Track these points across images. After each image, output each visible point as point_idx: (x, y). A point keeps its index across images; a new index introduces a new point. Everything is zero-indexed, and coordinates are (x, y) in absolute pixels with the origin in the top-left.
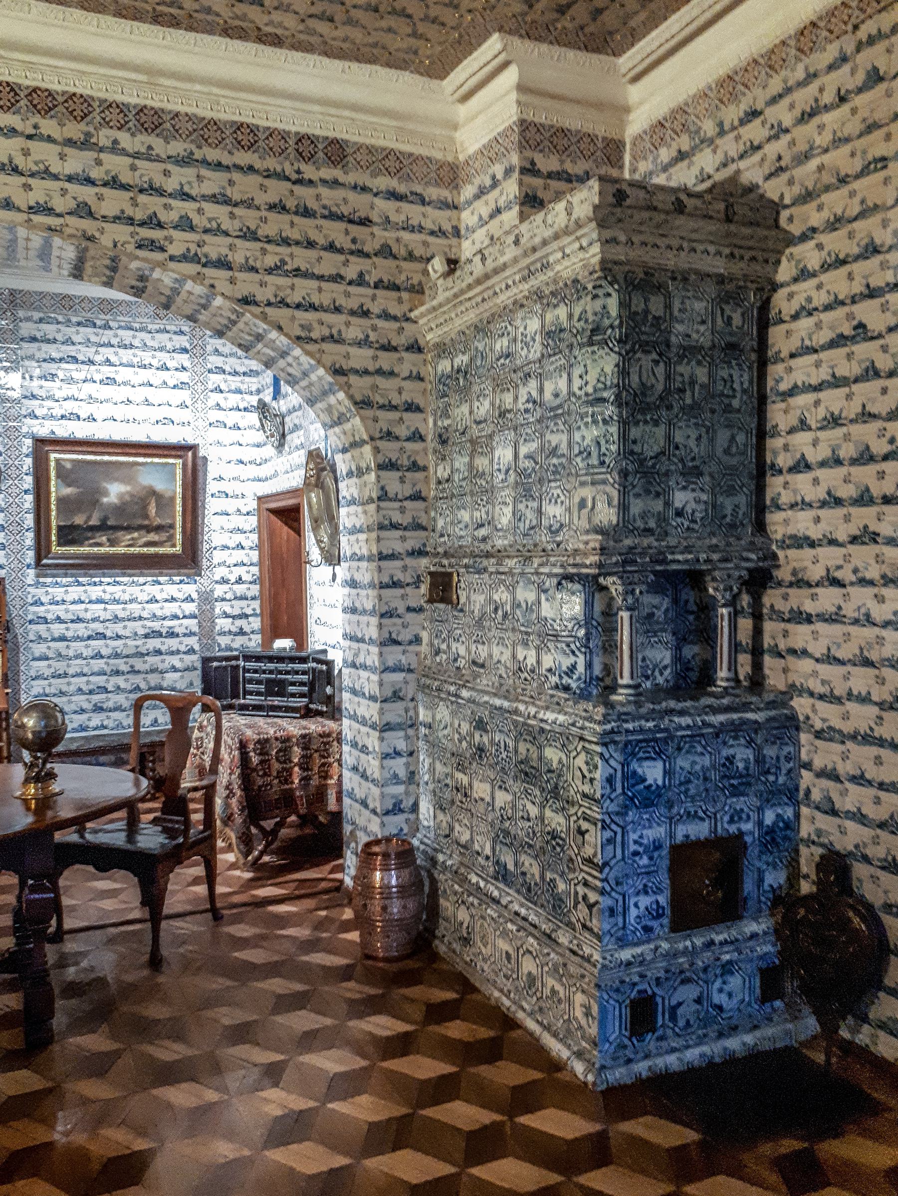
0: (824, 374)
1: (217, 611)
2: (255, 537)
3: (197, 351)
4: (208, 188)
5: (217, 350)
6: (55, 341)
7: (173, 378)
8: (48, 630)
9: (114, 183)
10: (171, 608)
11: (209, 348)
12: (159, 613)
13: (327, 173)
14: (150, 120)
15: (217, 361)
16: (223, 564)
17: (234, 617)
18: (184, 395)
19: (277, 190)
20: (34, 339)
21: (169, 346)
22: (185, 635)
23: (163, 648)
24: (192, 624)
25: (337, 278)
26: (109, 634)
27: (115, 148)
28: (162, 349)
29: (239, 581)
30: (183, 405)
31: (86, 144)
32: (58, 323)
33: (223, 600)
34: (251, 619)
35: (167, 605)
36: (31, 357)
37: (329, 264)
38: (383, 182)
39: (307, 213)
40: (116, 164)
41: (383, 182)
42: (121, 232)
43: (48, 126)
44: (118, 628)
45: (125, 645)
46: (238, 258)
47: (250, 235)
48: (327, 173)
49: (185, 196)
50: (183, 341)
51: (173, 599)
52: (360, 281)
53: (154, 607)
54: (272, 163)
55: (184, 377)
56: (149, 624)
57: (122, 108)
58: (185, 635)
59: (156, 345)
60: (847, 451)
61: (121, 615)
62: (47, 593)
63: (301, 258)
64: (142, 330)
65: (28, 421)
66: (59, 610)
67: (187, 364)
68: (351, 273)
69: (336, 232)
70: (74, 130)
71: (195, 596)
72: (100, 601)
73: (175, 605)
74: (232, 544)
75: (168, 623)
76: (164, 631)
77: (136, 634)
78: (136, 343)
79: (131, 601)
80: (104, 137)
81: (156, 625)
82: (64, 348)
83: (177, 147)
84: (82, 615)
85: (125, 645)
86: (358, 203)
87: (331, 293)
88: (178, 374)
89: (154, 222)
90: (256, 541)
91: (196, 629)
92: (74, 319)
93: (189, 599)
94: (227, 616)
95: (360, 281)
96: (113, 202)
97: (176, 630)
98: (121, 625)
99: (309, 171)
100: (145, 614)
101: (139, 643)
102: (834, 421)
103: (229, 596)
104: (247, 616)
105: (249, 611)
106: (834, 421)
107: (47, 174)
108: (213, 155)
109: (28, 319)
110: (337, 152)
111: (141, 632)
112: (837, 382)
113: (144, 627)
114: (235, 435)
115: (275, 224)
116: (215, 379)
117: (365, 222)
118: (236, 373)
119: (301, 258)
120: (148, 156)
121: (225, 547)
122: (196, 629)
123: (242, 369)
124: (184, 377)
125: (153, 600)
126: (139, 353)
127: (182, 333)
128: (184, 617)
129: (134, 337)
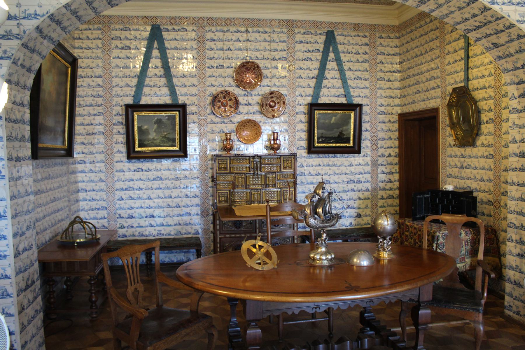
1: (379, 170)
2: (397, 134)
3: (373, 45)
5: (381, 44)
6: (310, 42)
7: (360, 58)
8: (306, 179)
10: (360, 169)
11: (378, 43)
12: (353, 171)
15: (381, 49)
16: (382, 147)
17: (386, 174)
18: (366, 65)
20: (301, 42)
21: (360, 43)
22: (365, 182)
23: (355, 189)
24: (368, 177)
26: (331, 181)
28: (357, 44)
29: (390, 156)
30: (366, 71)
32: (312, 34)
33: (382, 165)
34: (394, 174)
35: (357, 167)
36: (299, 50)
44: (336, 178)
45: (339, 187)
50: (366, 40)
51: (360, 164)
53: (352, 169)
55: (367, 57)
56: (349, 176)
58: (365, 182)
59: (354, 42)
61: (337, 172)
62: (305, 161)
64: (348, 36)
65: (298, 80)
66: (311, 169)
67: (368, 51)
71: (370, 163)
72: (328, 165)
73: (361, 167)
74: (386, 137)
75: (357, 176)
76: (355, 180)
77: (343, 181)
78: (345, 42)
79: (342, 165)
81: (352, 177)
82: (314, 45)
84: (320, 172)
85: (339, 187)
88: (363, 56)
90: (398, 136)
91: (369, 179)
92: (319, 32)
93: (367, 164)
94: (383, 173)
97: (361, 180)
98: (337, 177)
100: (347, 172)
101: (345, 185)
103: (385, 163)
104: (392, 173)
105: (394, 171)
109: (299, 33)
111: (346, 180)
113: (347, 178)
114: (388, 84)
116: (380, 58)
118: (389, 55)
121: (383, 139)
122: (369, 179)
123: (392, 53)
124: (367, 57)
125: (351, 165)
126: (346, 46)
127: (365, 36)
128: (365, 173)
129: (345, 39)
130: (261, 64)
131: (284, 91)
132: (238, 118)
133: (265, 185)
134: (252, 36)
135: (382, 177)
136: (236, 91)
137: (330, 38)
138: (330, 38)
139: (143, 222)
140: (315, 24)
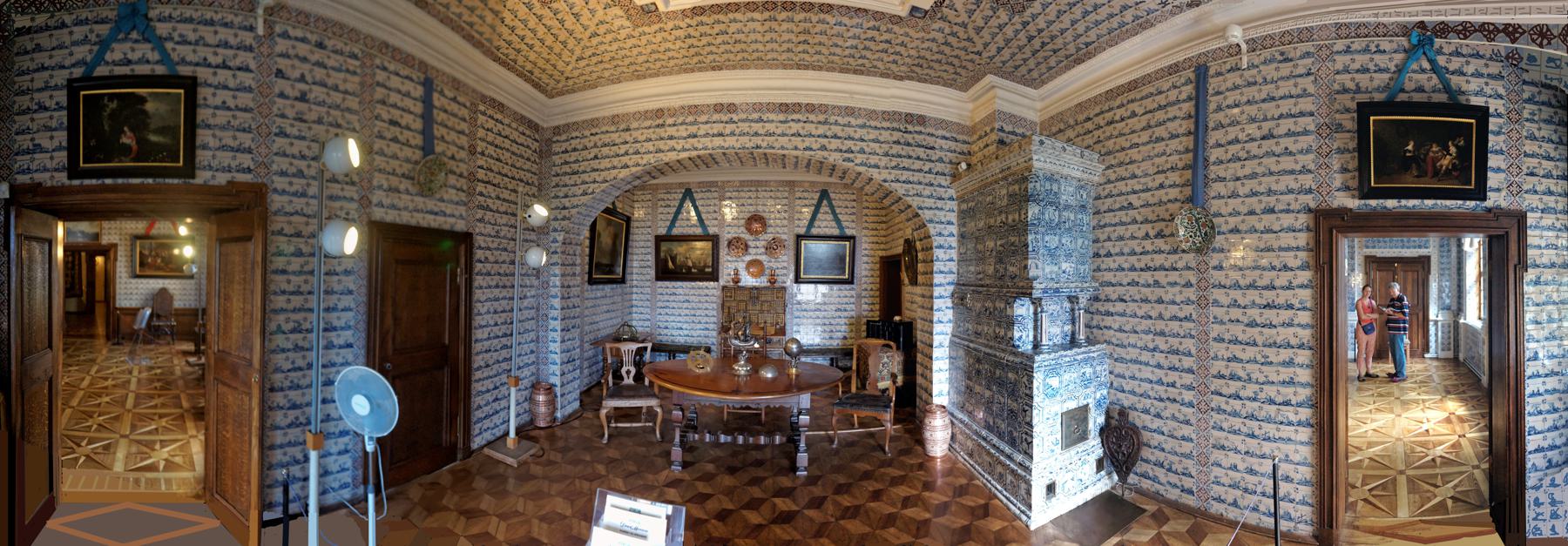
0: (1117, 220)
4: (872, 137)
9: (835, 137)
13: (918, 128)
14: (850, 111)
19: (897, 136)
25: (920, 171)
27: (836, 123)
31: (825, 122)
37: (917, 165)
38: (940, 133)
39: (909, 144)
40: (837, 130)
41: (940, 133)
42: (837, 156)
43: (812, 117)
46: (882, 164)
47: (886, 154)
48: (918, 128)
49: (863, 140)
52: (930, 172)
54: (895, 125)
57: (839, 108)
60: (1126, 250)
63: (906, 163)
68: (926, 168)
69: (921, 152)
70: (822, 118)
80: (832, 119)
83: (860, 121)
86: (930, 141)
87: (917, 177)
89: (850, 151)
95: (930, 172)
96: (835, 144)
99: (910, 128)
102: (1121, 238)
106: (1121, 238)
107: (811, 135)
108: (873, 123)
110: (922, 120)
112: (1122, 224)
115: (896, 149)
117: (932, 148)
119: (906, 163)
120: (849, 125)
130: (766, 215)
131: (784, 237)
132: (748, 258)
133: (762, 311)
134: (761, 194)
135: (865, 307)
136: (746, 236)
137: (824, 194)
138: (824, 194)
139: (675, 332)
140: (813, 183)
